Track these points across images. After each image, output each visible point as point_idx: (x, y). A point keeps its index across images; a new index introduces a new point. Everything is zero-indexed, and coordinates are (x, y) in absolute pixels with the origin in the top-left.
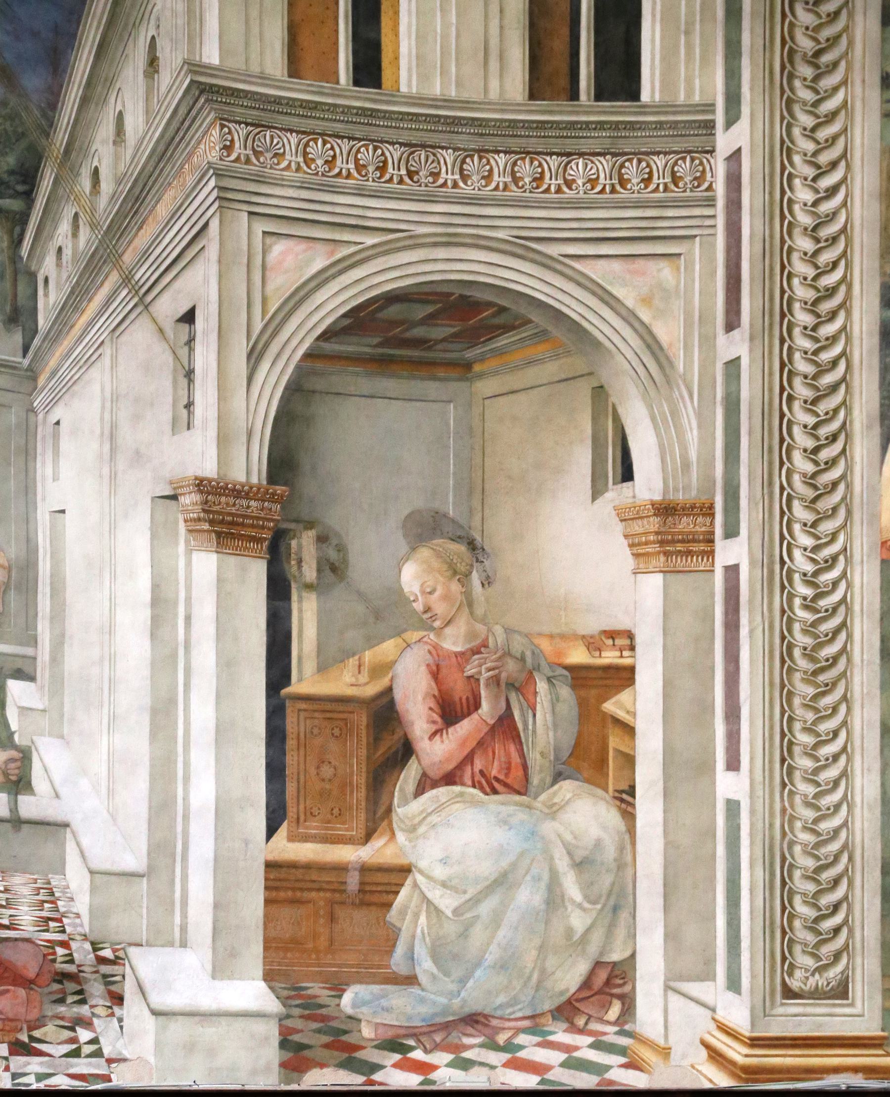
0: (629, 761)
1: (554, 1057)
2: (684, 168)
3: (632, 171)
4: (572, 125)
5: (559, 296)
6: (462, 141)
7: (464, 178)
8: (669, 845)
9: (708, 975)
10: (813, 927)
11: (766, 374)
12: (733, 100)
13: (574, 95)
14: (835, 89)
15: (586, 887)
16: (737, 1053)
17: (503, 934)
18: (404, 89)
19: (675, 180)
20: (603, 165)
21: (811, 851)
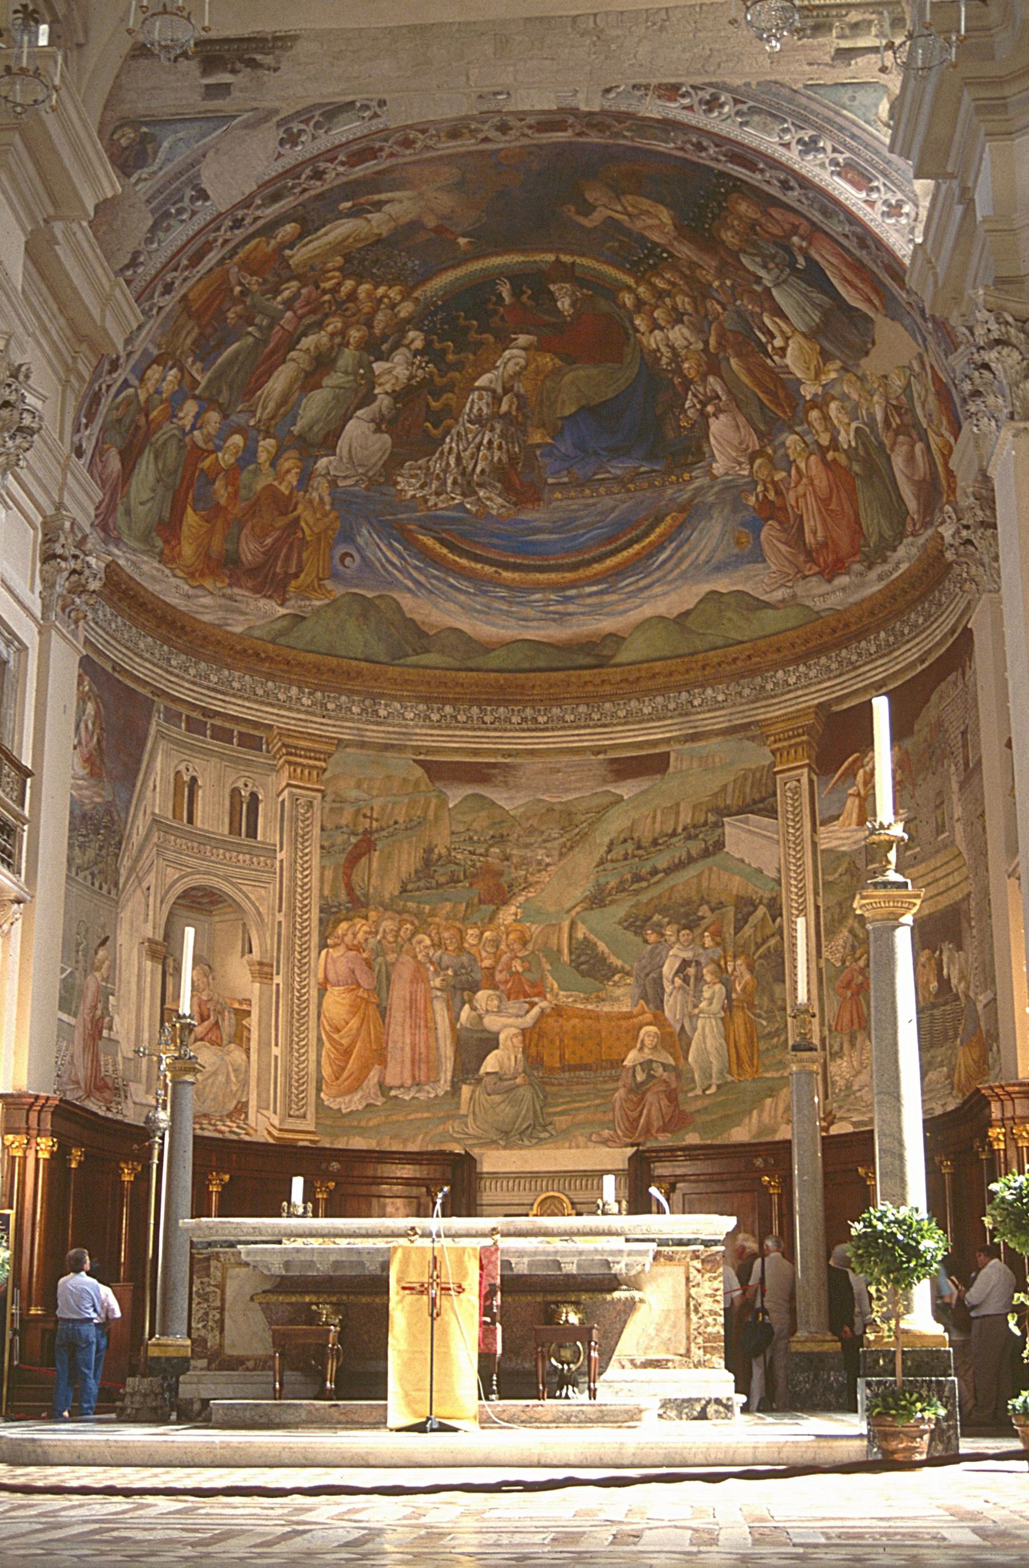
0: (249, 1039)
1: (227, 1129)
3: (255, 860)
8: (259, 1067)
9: (268, 1109)
10: (297, 1096)
11: (288, 927)
15: (237, 1077)
16: (276, 1133)
17: (214, 1090)
20: (248, 857)
21: (297, 1073)
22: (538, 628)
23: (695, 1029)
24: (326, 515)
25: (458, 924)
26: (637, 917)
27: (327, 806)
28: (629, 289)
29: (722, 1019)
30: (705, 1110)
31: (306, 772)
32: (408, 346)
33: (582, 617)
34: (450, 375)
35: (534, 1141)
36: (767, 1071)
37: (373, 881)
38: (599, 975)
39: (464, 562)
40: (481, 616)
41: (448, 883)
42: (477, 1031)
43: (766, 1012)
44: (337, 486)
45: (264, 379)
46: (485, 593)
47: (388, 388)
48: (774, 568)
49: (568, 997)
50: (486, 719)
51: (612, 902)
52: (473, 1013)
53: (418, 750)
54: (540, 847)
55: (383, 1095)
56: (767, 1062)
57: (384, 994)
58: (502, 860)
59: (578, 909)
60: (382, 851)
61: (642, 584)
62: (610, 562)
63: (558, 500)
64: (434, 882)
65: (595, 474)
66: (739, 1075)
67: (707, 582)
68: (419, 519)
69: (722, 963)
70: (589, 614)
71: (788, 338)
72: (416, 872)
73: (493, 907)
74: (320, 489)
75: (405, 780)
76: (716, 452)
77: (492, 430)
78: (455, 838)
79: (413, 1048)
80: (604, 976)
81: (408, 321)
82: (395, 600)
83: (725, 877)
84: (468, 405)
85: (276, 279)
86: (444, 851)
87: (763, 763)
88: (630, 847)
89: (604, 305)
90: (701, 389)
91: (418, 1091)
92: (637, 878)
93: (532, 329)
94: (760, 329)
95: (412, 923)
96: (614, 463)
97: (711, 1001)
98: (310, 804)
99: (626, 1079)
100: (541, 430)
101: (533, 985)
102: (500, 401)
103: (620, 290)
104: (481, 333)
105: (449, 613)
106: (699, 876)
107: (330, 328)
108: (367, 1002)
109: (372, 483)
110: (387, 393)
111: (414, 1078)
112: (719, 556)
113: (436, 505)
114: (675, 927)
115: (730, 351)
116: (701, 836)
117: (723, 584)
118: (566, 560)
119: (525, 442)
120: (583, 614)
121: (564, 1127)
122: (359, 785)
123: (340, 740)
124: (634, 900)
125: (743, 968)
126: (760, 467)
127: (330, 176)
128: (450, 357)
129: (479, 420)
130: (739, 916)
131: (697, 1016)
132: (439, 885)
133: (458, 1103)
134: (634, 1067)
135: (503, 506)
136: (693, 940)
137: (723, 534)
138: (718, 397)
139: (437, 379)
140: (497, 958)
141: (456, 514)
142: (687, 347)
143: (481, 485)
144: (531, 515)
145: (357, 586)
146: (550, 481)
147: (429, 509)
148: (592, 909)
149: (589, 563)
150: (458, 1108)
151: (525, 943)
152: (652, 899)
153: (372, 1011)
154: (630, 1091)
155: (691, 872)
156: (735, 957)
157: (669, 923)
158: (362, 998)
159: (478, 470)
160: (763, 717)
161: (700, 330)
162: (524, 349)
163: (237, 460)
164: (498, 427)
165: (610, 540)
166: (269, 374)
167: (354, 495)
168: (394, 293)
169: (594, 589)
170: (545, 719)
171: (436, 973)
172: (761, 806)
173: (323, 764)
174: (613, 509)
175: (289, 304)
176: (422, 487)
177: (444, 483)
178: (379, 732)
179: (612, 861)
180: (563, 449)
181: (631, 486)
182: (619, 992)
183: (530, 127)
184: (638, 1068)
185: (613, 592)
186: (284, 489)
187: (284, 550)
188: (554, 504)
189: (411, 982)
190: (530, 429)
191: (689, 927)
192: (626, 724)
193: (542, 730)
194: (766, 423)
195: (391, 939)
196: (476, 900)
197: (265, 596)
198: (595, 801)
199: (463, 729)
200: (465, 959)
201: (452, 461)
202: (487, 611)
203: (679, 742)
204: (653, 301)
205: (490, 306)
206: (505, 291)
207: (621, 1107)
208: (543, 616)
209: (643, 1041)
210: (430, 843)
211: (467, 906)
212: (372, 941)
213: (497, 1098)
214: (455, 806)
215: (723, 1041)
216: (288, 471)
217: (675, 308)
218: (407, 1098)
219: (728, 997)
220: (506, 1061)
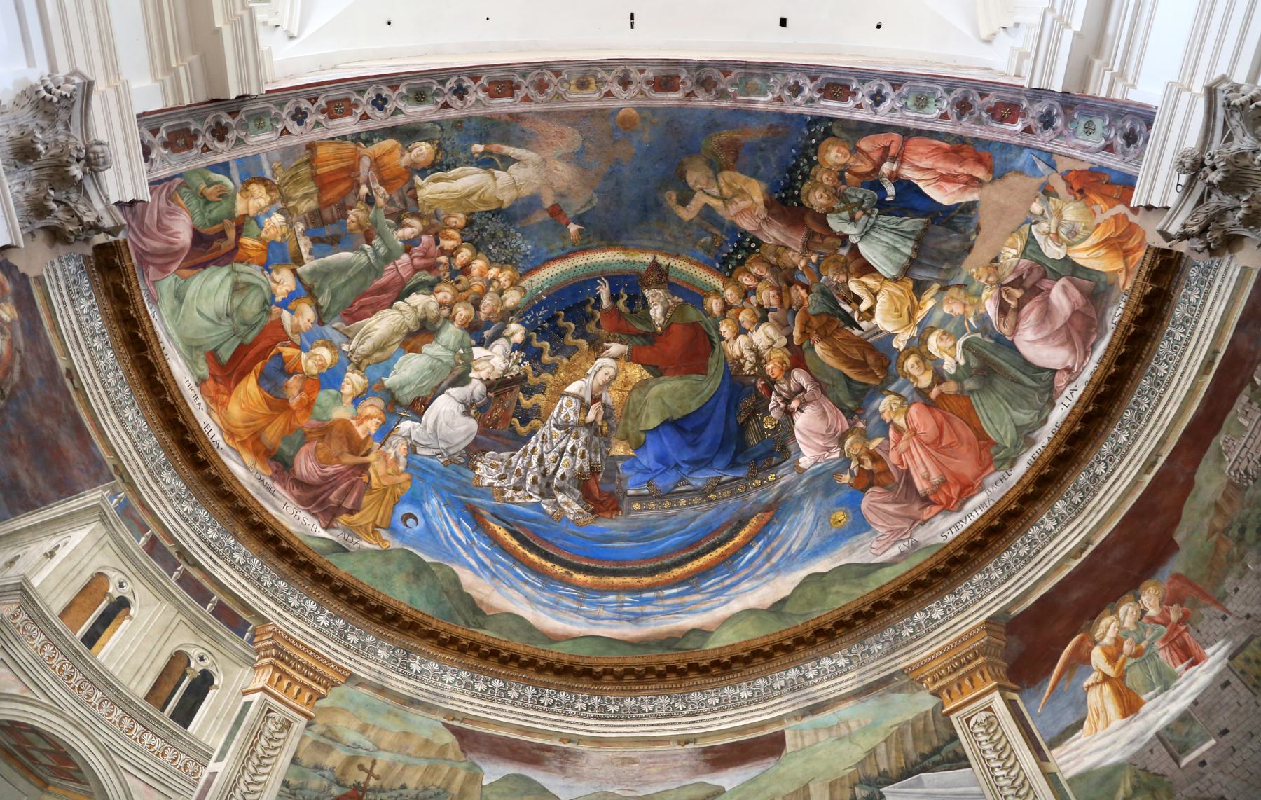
2: (191, 765)
3: (169, 752)
4: (155, 720)
5: (109, 782)
6: (108, 693)
7: (100, 707)
12: (223, 753)
13: (163, 710)
14: (264, 774)
18: (99, 657)
19: (185, 767)
20: (159, 743)
22: (610, 626)
24: (398, 473)
27: (311, 736)
28: (717, 292)
31: (296, 688)
32: (508, 338)
33: (660, 617)
34: (542, 375)
39: (534, 557)
40: (547, 610)
44: (415, 452)
45: (369, 311)
46: (553, 590)
47: (484, 375)
48: (882, 531)
50: (542, 700)
53: (452, 715)
61: (728, 582)
62: (691, 566)
63: (637, 510)
65: (675, 487)
67: (803, 568)
68: (493, 507)
70: (669, 613)
71: (875, 295)
74: (397, 448)
75: (427, 743)
76: (801, 446)
77: (577, 437)
81: (512, 312)
82: (454, 572)
84: (557, 410)
85: (402, 206)
87: (924, 710)
89: (692, 314)
90: (785, 387)
93: (624, 337)
94: (845, 300)
96: (695, 475)
98: (287, 725)
100: (625, 442)
102: (588, 409)
103: (708, 296)
104: (576, 338)
105: (511, 599)
107: (440, 296)
109: (451, 460)
110: (481, 379)
112: (815, 540)
113: (512, 498)
115: (814, 337)
117: (822, 565)
118: (642, 566)
119: (608, 452)
120: (662, 613)
122: (363, 729)
123: (352, 675)
126: (852, 444)
127: (471, 98)
128: (546, 358)
129: (565, 427)
135: (580, 513)
137: (817, 520)
138: (803, 389)
139: (530, 376)
141: (531, 512)
142: (770, 347)
143: (560, 490)
144: (607, 525)
145: (414, 547)
146: (630, 492)
147: (504, 501)
149: (668, 568)
159: (559, 474)
160: (906, 664)
161: (784, 326)
162: (616, 359)
163: (320, 374)
164: (583, 435)
165: (692, 545)
166: (375, 308)
167: (431, 467)
168: (505, 277)
169: (674, 591)
170: (617, 708)
173: (323, 691)
174: (694, 518)
175: (409, 245)
176: (502, 478)
177: (524, 480)
178: (407, 684)
180: (645, 462)
181: (713, 496)
183: (648, 82)
185: (696, 593)
186: (360, 431)
187: (344, 486)
188: (633, 514)
190: (613, 441)
192: (719, 711)
193: (611, 719)
194: (855, 398)
197: (308, 511)
199: (513, 704)
201: (534, 460)
202: (554, 606)
203: (796, 718)
204: (738, 303)
205: (589, 309)
206: (604, 291)
208: (617, 616)
214: (491, 784)
216: (369, 417)
217: (760, 306)
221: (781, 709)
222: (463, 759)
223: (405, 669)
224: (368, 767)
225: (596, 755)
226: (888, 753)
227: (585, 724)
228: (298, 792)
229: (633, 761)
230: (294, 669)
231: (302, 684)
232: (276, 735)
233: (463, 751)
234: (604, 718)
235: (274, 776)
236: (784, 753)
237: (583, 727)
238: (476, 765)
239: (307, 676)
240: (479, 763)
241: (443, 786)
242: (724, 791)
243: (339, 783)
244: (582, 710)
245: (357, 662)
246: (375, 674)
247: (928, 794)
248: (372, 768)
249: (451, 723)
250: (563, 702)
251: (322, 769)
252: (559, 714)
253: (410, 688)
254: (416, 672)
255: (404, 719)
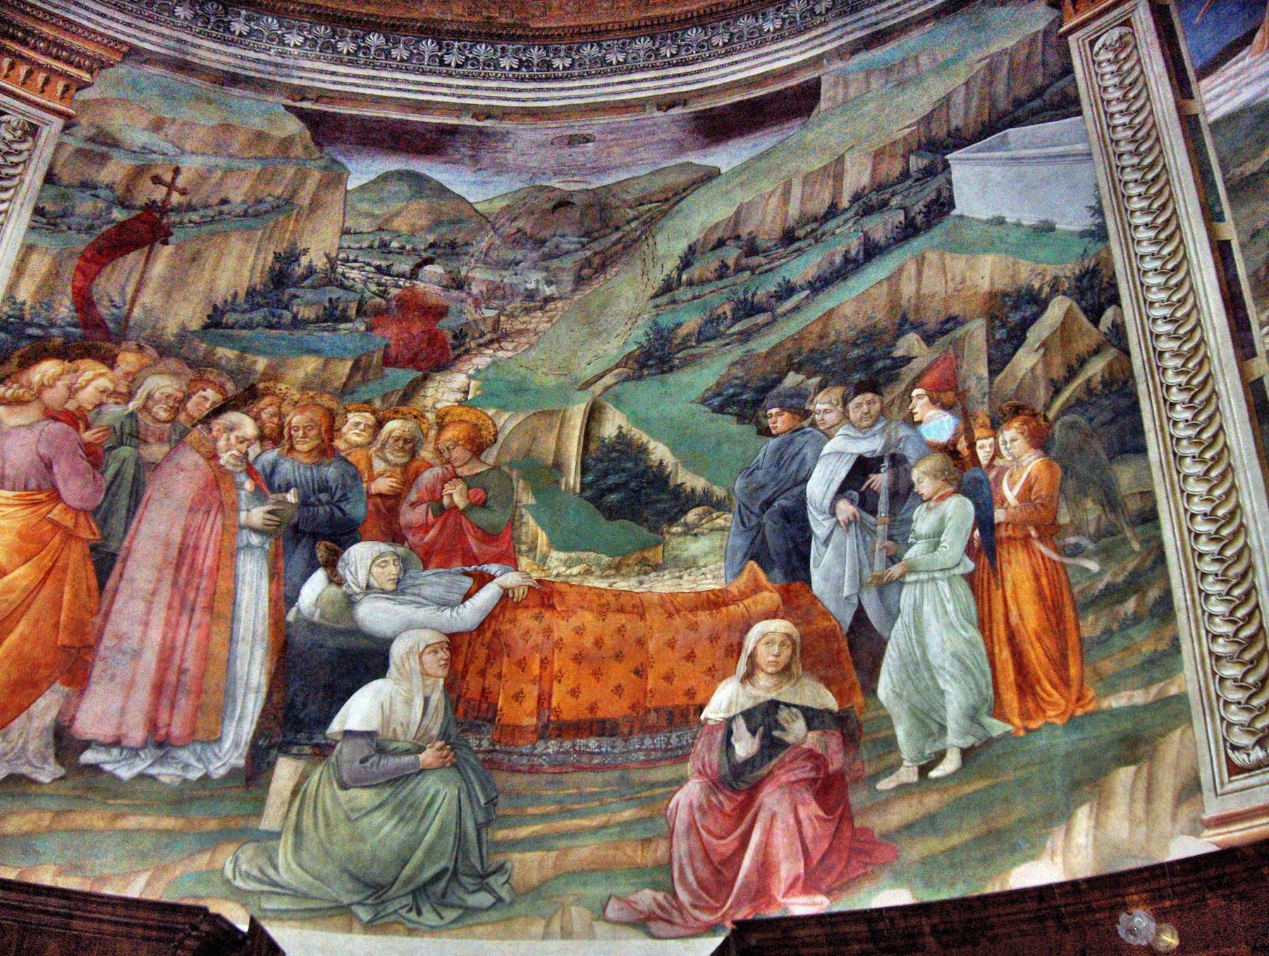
23: (892, 615)
25: (326, 401)
26: (744, 386)
29: (970, 578)
30: (928, 824)
31: (41, 77)
35: (450, 915)
36: (1111, 687)
37: (147, 298)
38: (647, 513)
41: (318, 320)
42: (340, 632)
43: (1097, 537)
49: (569, 564)
50: (447, 59)
51: (685, 363)
52: (334, 588)
53: (301, 93)
54: (535, 267)
55: (60, 758)
56: (1108, 666)
57: (116, 524)
58: (446, 288)
59: (608, 380)
60: (178, 247)
64: (288, 315)
66: (1025, 715)
69: (962, 446)
72: (251, 293)
73: (415, 374)
75: (260, 136)
78: (347, 241)
79: (166, 655)
80: (664, 512)
83: (958, 264)
86: (320, 263)
88: (731, 254)
91: (159, 761)
92: (748, 308)
95: (221, 389)
97: (935, 539)
98: (32, 131)
99: (706, 753)
101: (488, 536)
106: (894, 279)
108: (70, 536)
111: (153, 725)
114: (836, 393)
116: (894, 202)
121: (534, 878)
122: (157, 126)
124: (738, 352)
125: (1020, 445)
130: (1000, 334)
131: (900, 583)
132: (297, 323)
133: (261, 802)
134: (730, 721)
136: (882, 412)
140: (409, 476)
148: (640, 378)
150: (259, 814)
151: (477, 446)
152: (781, 344)
153: (76, 554)
154: (716, 784)
155: (877, 272)
156: (995, 426)
157: (821, 387)
158: (56, 525)
170: (568, 62)
171: (259, 496)
172: (1036, 103)
173: (86, 77)
179: (690, 283)
182: (696, 547)
184: (740, 727)
189: (192, 510)
191: (872, 386)
192: (727, 54)
193: (556, 79)
195: (163, 415)
196: (377, 358)
198: (660, 182)
199: (398, 69)
200: (331, 472)
207: (692, 827)
209: (752, 656)
210: (293, 245)
211: (356, 367)
212: (114, 412)
213: (364, 797)
214: (362, 188)
215: (973, 633)
218: (125, 773)
219: (984, 522)
220: (400, 707)
221: (822, 45)
222: (318, 155)
223: (224, 35)
224: (168, 177)
225: (526, 135)
226: (967, 100)
227: (514, 90)
228: (59, 221)
229: (586, 139)
230: (35, 48)
231: (50, 70)
232: (15, 146)
233: (317, 144)
234: (547, 79)
235: (18, 204)
236: (815, 112)
237: (510, 95)
238: (335, 161)
239: (57, 58)
240: (341, 159)
241: (286, 196)
242: (720, 174)
243: (123, 204)
244: (512, 69)
245: (141, 29)
246: (172, 43)
247: (1013, 159)
248: (174, 179)
249: (299, 104)
250: (481, 59)
251: (95, 188)
252: (474, 78)
253: (231, 60)
254: (241, 35)
255: (221, 105)
